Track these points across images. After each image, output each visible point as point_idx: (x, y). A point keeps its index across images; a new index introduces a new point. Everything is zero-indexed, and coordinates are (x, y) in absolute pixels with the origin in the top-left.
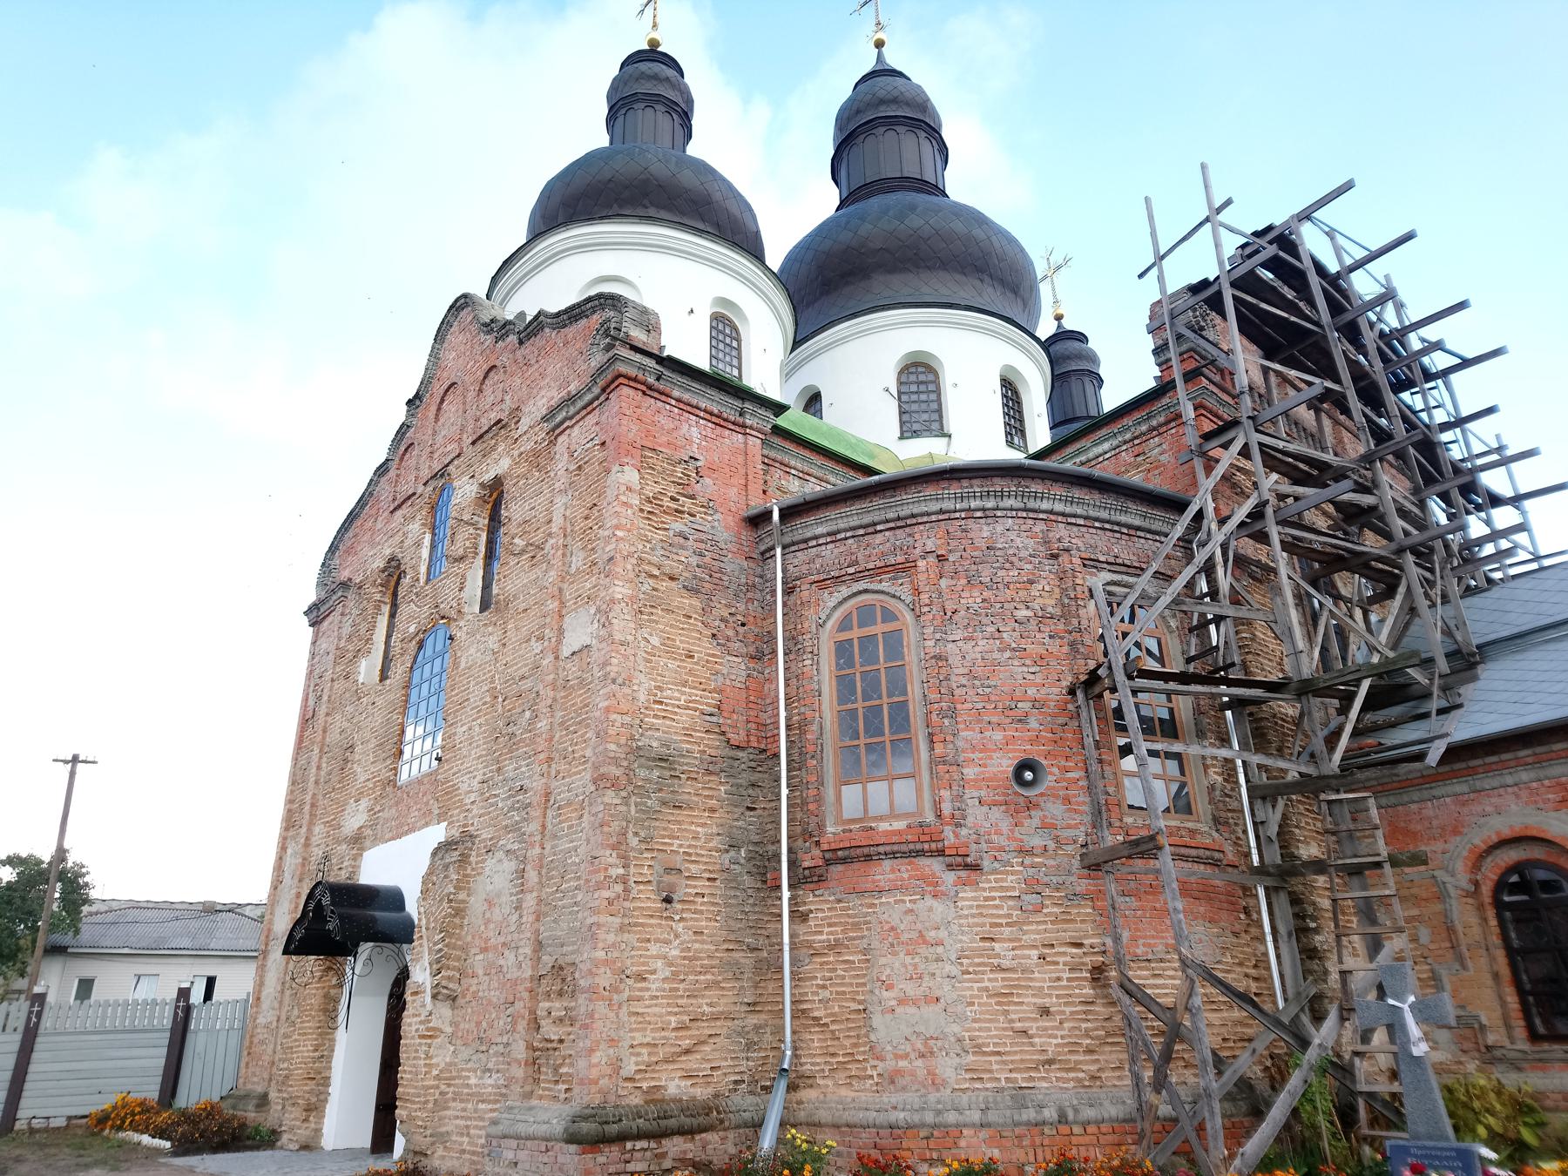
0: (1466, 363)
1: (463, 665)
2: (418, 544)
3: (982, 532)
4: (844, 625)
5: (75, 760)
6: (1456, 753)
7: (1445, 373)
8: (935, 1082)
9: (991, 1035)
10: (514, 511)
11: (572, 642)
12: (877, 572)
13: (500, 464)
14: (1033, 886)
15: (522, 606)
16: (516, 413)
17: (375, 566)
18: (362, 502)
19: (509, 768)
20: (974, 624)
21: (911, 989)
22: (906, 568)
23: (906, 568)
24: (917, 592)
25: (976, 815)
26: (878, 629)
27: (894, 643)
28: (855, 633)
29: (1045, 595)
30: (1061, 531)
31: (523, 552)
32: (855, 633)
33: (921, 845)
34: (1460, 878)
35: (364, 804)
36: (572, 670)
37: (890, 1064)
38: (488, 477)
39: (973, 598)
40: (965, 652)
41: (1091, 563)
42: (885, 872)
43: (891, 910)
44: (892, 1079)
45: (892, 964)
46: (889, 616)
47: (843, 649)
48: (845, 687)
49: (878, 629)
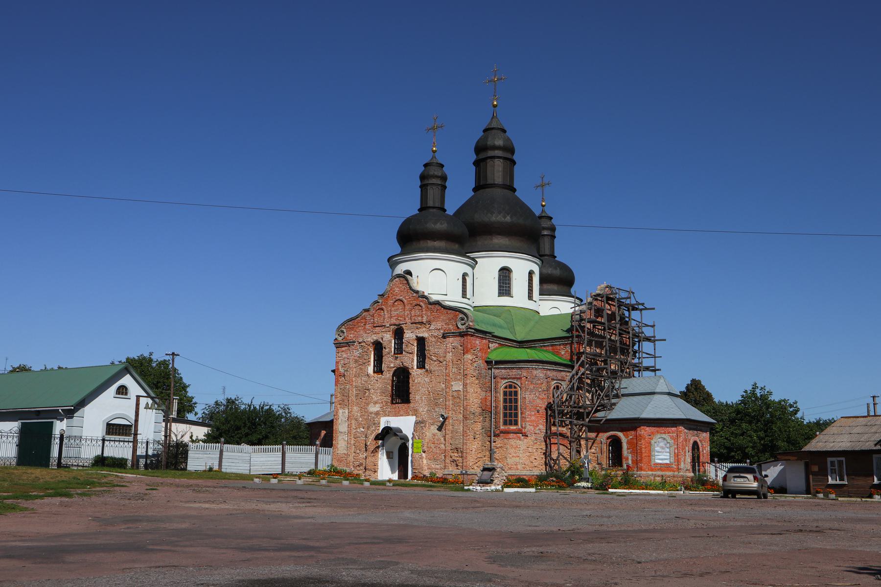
0: (646, 309)
2: (390, 342)
3: (535, 372)
4: (506, 387)
5: (173, 354)
6: (607, 420)
7: (641, 310)
10: (432, 349)
11: (455, 388)
12: (514, 378)
14: (536, 439)
16: (429, 323)
18: (357, 317)
19: (437, 409)
20: (531, 391)
22: (520, 378)
23: (520, 378)
25: (528, 427)
26: (513, 390)
27: (516, 393)
28: (508, 390)
29: (544, 386)
30: (549, 372)
32: (508, 390)
33: (519, 432)
34: (604, 441)
35: (377, 405)
36: (455, 394)
39: (532, 387)
40: (529, 396)
41: (553, 380)
42: (511, 435)
43: (512, 442)
46: (515, 387)
47: (505, 394)
48: (505, 401)
49: (513, 390)
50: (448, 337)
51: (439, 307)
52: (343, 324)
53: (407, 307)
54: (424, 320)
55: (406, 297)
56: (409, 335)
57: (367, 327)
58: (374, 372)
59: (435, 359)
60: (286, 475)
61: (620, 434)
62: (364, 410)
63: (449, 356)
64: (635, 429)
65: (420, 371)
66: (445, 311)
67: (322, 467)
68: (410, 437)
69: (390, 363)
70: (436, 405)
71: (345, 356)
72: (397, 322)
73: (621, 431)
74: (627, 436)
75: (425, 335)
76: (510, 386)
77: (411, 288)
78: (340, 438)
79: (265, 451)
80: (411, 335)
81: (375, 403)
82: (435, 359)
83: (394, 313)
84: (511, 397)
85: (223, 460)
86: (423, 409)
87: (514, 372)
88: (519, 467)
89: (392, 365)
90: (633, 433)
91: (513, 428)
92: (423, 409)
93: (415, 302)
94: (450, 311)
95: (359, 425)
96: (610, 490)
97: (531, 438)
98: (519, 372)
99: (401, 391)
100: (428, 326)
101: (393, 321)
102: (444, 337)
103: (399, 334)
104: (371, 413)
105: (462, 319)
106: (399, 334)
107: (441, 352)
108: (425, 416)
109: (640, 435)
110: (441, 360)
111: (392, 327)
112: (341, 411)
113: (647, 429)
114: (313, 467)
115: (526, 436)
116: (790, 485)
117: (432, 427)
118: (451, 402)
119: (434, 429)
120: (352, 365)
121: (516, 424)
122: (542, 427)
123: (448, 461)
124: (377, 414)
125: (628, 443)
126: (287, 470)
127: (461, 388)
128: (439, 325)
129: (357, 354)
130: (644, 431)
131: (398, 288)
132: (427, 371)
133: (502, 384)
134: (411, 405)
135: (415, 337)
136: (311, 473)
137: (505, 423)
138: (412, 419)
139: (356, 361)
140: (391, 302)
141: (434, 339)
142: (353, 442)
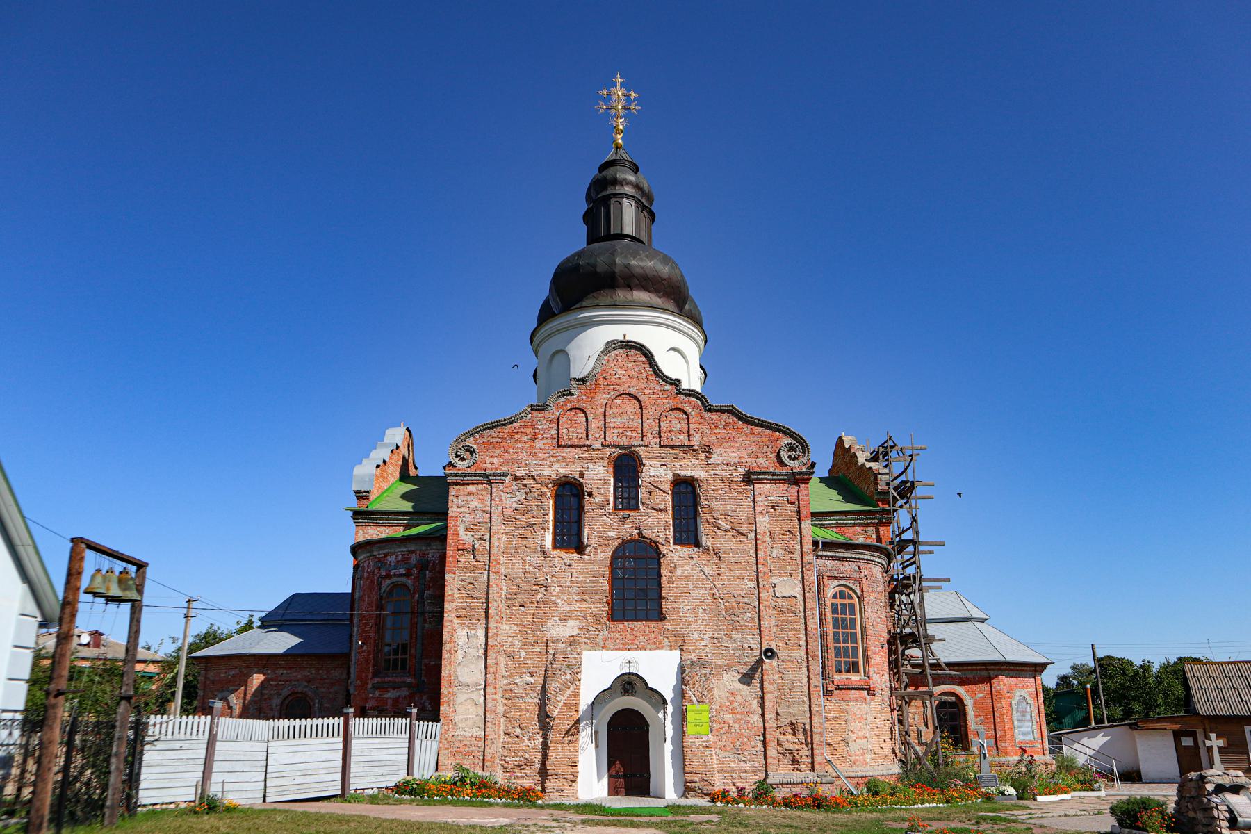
1: (679, 572)
2: (606, 482)
4: (835, 597)
8: (866, 763)
9: (877, 750)
10: (719, 503)
12: (850, 579)
13: (691, 468)
15: (733, 560)
17: (546, 473)
19: (735, 636)
21: (860, 734)
24: (862, 590)
26: (847, 601)
27: (852, 606)
28: (838, 601)
31: (726, 531)
35: (571, 623)
36: (781, 603)
37: (853, 758)
38: (682, 473)
42: (852, 694)
43: (855, 708)
44: (853, 763)
45: (854, 725)
49: (847, 601)
50: (760, 481)
51: (731, 419)
52: (470, 434)
53: (648, 413)
54: (695, 442)
55: (647, 389)
56: (657, 472)
57: (539, 444)
58: (555, 547)
59: (726, 526)
60: (356, 800)
61: (959, 690)
62: (531, 630)
63: (763, 523)
64: (988, 680)
65: (685, 551)
66: (747, 428)
67: (424, 770)
68: (669, 695)
69: (604, 528)
70: (736, 625)
71: (474, 504)
72: (624, 441)
73: (962, 682)
74: (973, 694)
75: (699, 473)
76: (842, 595)
77: (658, 372)
78: (461, 698)
79: (302, 734)
80: (662, 471)
81: (566, 617)
82: (726, 526)
83: (613, 421)
84: (845, 615)
85: (216, 767)
86: (701, 637)
87: (848, 566)
88: (868, 758)
89: (612, 534)
90: (984, 687)
91: (854, 678)
92: (701, 637)
93: (668, 404)
94: (758, 430)
95: (518, 666)
96: (1040, 798)
97: (878, 699)
98: (853, 566)
99: (636, 593)
100: (702, 456)
101: (612, 437)
102: (748, 479)
103: (627, 468)
104: (556, 641)
105: (791, 449)
106: (627, 468)
107: (742, 510)
108: (708, 652)
109: (998, 692)
110: (743, 529)
111: (609, 450)
112: (461, 634)
113: (1006, 680)
114: (401, 776)
115: (871, 692)
116: (1146, 768)
117: (726, 676)
118: (773, 622)
119: (730, 680)
120: (498, 526)
121: (856, 671)
122: (886, 677)
123: (772, 752)
124: (572, 642)
125: (976, 704)
126: (355, 783)
127: (797, 591)
128: (733, 456)
129: (510, 503)
130: (1003, 683)
131: (626, 370)
132: (706, 550)
133: (831, 589)
134: (668, 625)
135: (670, 477)
136: (401, 788)
137: (840, 671)
138: (674, 657)
139: (507, 520)
140: (602, 397)
141: (719, 484)
142: (501, 709)
